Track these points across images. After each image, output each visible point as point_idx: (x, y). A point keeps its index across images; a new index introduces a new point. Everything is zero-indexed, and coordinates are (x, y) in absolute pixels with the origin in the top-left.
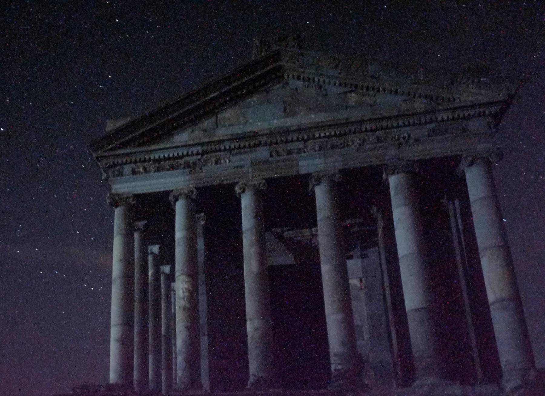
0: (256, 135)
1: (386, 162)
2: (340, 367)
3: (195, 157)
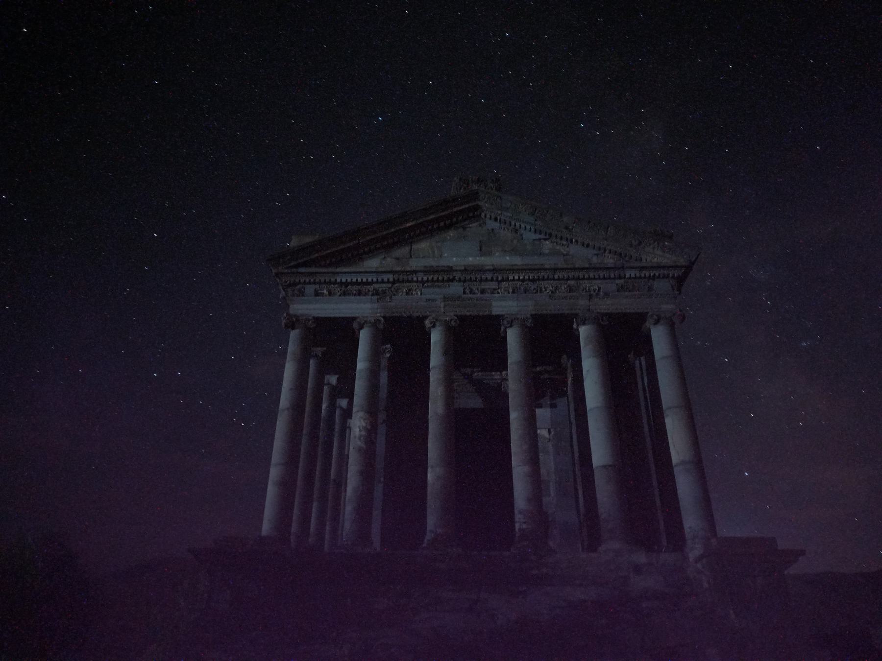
0: (450, 270)
1: (577, 311)
2: (524, 526)
3: (384, 285)
